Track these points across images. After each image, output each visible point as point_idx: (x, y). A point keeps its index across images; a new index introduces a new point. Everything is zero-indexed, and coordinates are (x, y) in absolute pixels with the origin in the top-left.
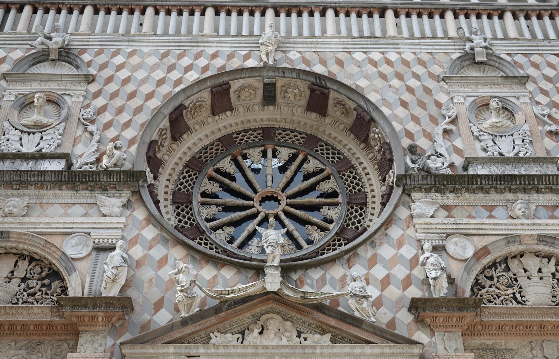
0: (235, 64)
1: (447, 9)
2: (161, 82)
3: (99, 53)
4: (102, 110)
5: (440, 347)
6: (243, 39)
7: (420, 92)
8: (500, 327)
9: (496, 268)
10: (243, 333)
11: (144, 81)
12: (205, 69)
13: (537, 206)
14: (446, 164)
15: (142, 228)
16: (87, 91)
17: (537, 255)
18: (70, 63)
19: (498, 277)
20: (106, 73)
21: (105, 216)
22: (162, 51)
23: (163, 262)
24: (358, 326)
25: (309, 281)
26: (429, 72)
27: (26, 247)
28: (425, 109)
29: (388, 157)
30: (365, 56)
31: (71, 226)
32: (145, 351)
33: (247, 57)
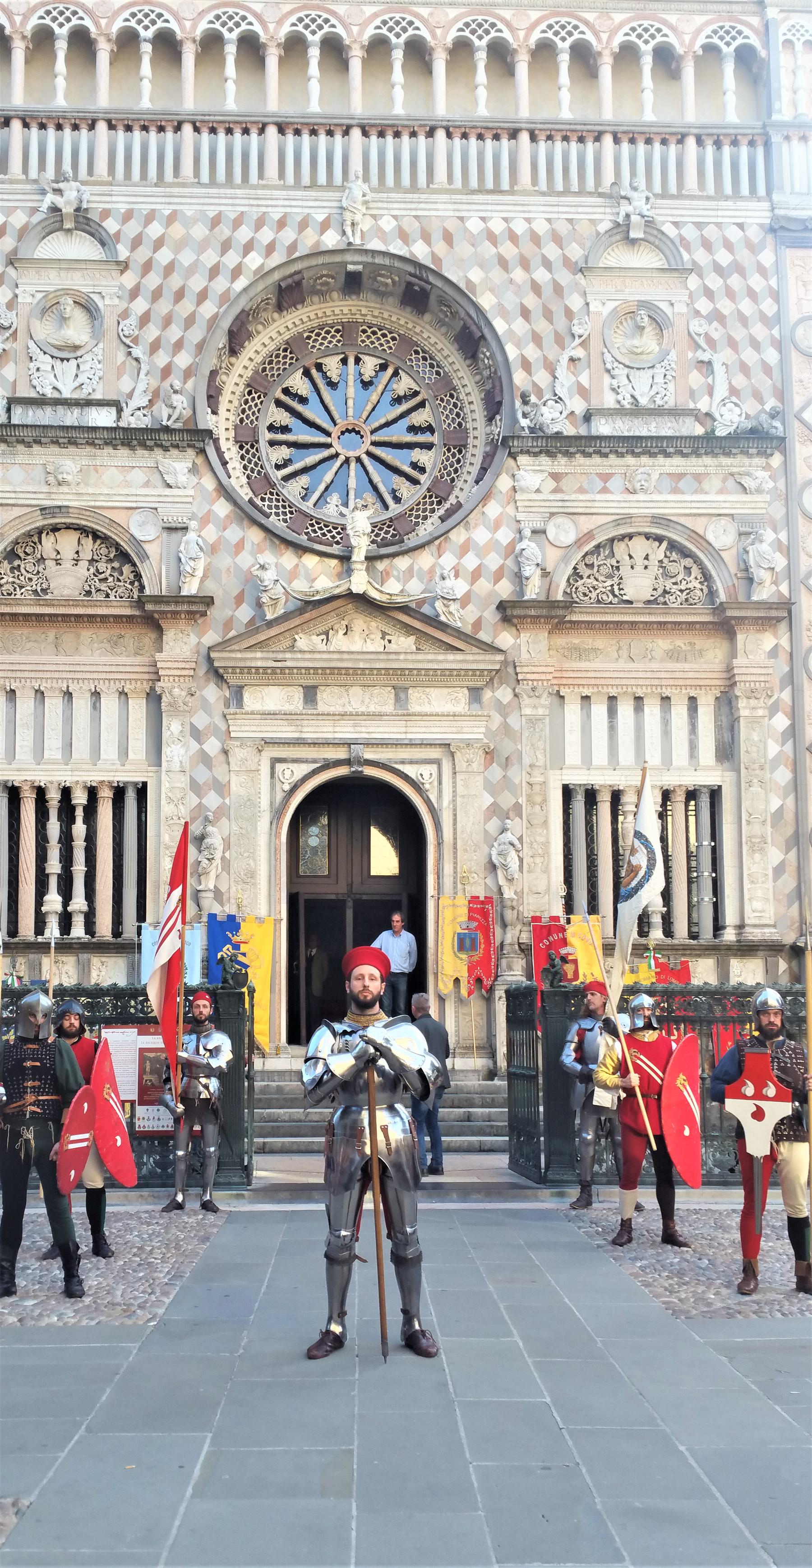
0: (309, 241)
1: (606, 132)
2: (214, 272)
3: (128, 216)
4: (145, 319)
5: (524, 650)
6: (319, 194)
7: (548, 291)
8: (590, 625)
9: (599, 554)
10: (327, 634)
11: (192, 270)
12: (270, 248)
13: (661, 474)
14: (565, 414)
15: (213, 503)
16: (121, 287)
17: (648, 537)
18: (92, 235)
19: (599, 566)
20: (143, 253)
21: (169, 486)
22: (211, 214)
23: (239, 546)
24: (442, 631)
25: (395, 573)
26: (564, 255)
27: (89, 524)
28: (551, 322)
29: (498, 399)
30: (482, 225)
31: (134, 499)
32: (233, 655)
33: (325, 226)
